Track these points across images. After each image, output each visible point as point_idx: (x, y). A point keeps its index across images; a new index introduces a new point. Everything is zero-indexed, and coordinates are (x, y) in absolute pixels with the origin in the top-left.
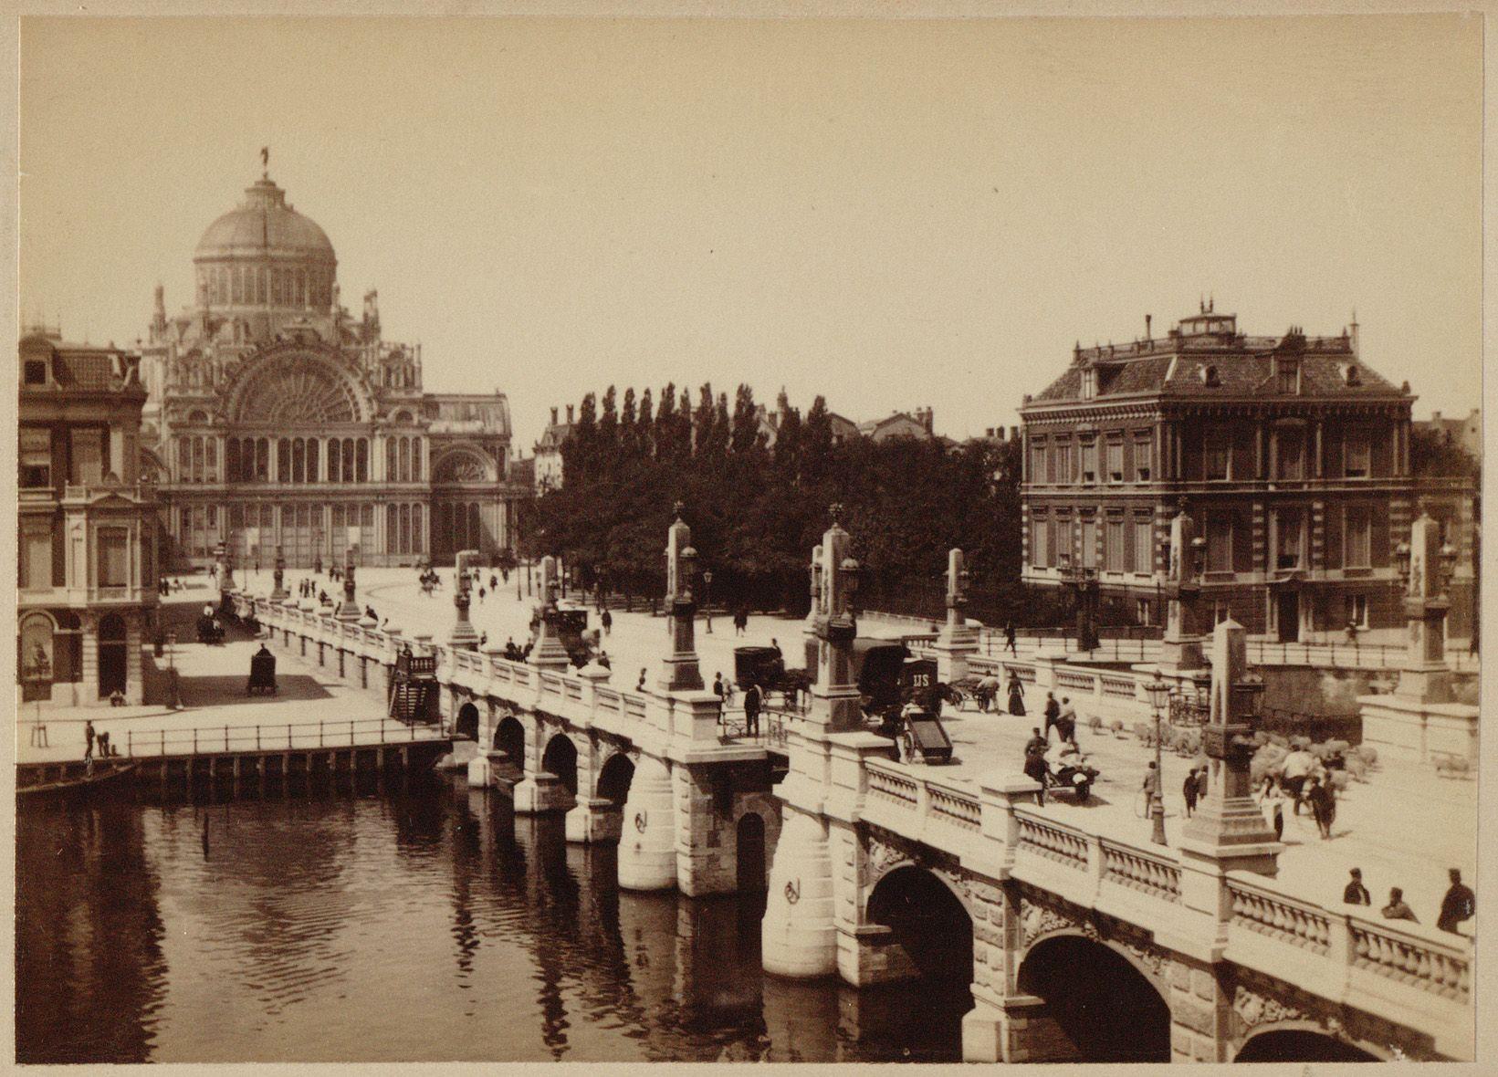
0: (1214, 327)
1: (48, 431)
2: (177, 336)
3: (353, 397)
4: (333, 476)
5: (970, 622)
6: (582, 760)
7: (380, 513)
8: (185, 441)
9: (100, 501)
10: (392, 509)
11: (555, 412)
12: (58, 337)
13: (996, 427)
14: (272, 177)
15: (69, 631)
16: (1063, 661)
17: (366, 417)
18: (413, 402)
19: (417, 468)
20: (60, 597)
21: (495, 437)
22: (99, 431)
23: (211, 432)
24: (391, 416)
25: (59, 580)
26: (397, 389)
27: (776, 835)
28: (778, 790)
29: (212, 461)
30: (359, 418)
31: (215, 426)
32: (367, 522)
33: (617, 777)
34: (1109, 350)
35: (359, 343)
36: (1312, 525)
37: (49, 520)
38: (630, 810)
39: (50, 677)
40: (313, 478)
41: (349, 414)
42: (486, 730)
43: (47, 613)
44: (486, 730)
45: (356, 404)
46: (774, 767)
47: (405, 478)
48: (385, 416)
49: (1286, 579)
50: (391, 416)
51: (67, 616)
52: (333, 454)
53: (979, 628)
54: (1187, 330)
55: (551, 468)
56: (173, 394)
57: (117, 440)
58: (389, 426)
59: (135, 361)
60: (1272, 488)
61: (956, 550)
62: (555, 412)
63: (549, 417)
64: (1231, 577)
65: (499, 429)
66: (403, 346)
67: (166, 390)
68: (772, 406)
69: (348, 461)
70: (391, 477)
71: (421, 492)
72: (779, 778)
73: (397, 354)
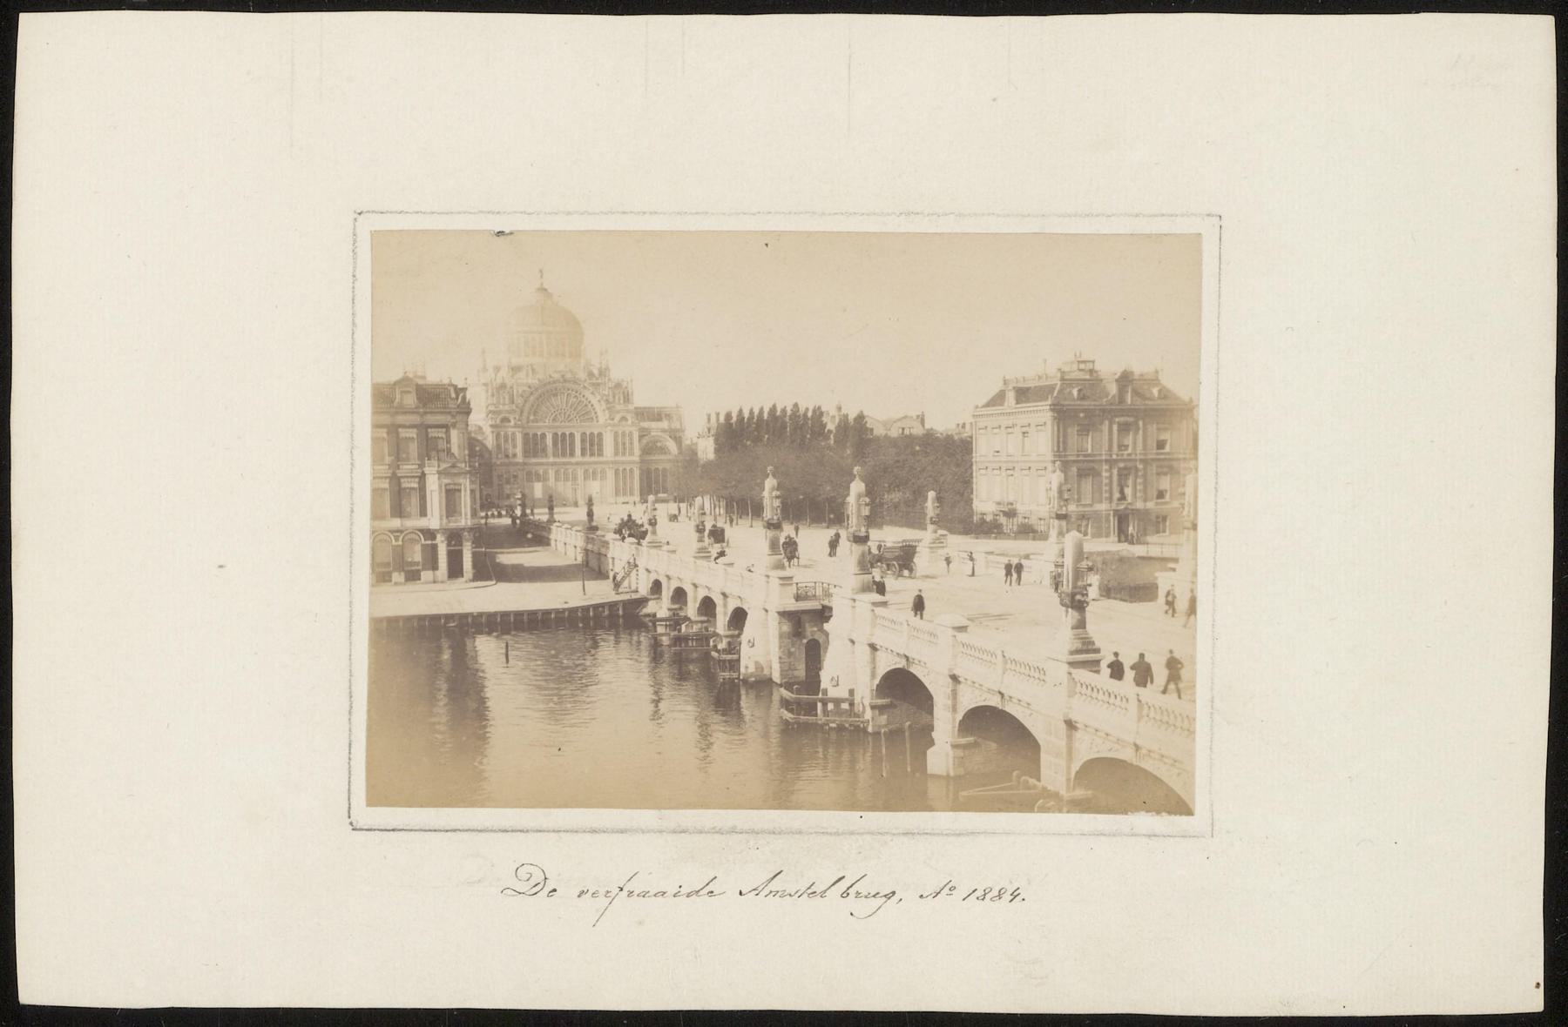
0: (1082, 366)
1: (415, 430)
2: (493, 376)
3: (594, 409)
4: (583, 454)
5: (941, 532)
6: (719, 610)
7: (610, 474)
8: (498, 435)
9: (446, 469)
10: (617, 472)
11: (709, 416)
12: (424, 378)
13: (961, 422)
14: (545, 286)
15: (430, 542)
16: (992, 553)
17: (602, 420)
18: (628, 411)
19: (632, 449)
20: (423, 523)
21: (676, 431)
22: (444, 430)
23: (513, 430)
24: (616, 421)
25: (423, 513)
26: (620, 404)
27: (827, 648)
28: (826, 626)
29: (515, 446)
30: (597, 421)
31: (516, 426)
32: (603, 478)
33: (739, 617)
34: (1022, 380)
35: (597, 379)
36: (1136, 477)
37: (417, 480)
38: (745, 638)
39: (420, 567)
40: (572, 454)
41: (592, 418)
42: (667, 594)
43: (419, 533)
44: (667, 594)
45: (596, 413)
46: (824, 614)
47: (624, 454)
48: (613, 419)
49: (1122, 507)
50: (616, 421)
51: (429, 534)
52: (583, 441)
53: (945, 535)
54: (1066, 369)
55: (707, 450)
56: (492, 408)
57: (454, 433)
58: (614, 425)
59: (464, 390)
60: (1114, 457)
61: (932, 492)
62: (709, 416)
63: (706, 418)
64: (1091, 505)
65: (678, 427)
66: (623, 381)
67: (487, 407)
68: (833, 412)
69: (592, 445)
70: (616, 454)
71: (633, 462)
72: (827, 619)
73: (618, 385)
